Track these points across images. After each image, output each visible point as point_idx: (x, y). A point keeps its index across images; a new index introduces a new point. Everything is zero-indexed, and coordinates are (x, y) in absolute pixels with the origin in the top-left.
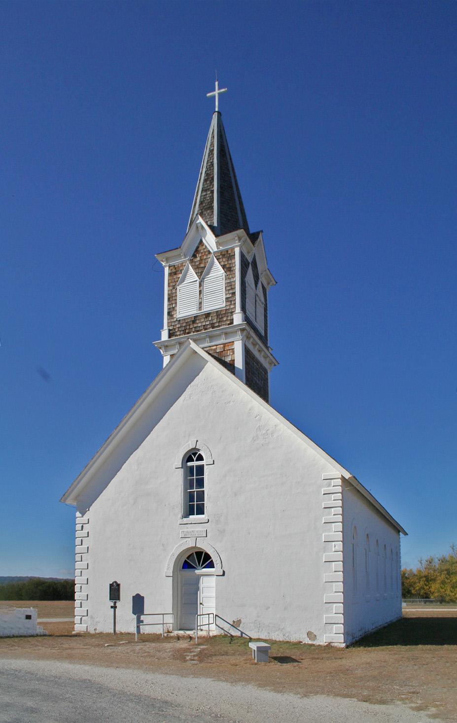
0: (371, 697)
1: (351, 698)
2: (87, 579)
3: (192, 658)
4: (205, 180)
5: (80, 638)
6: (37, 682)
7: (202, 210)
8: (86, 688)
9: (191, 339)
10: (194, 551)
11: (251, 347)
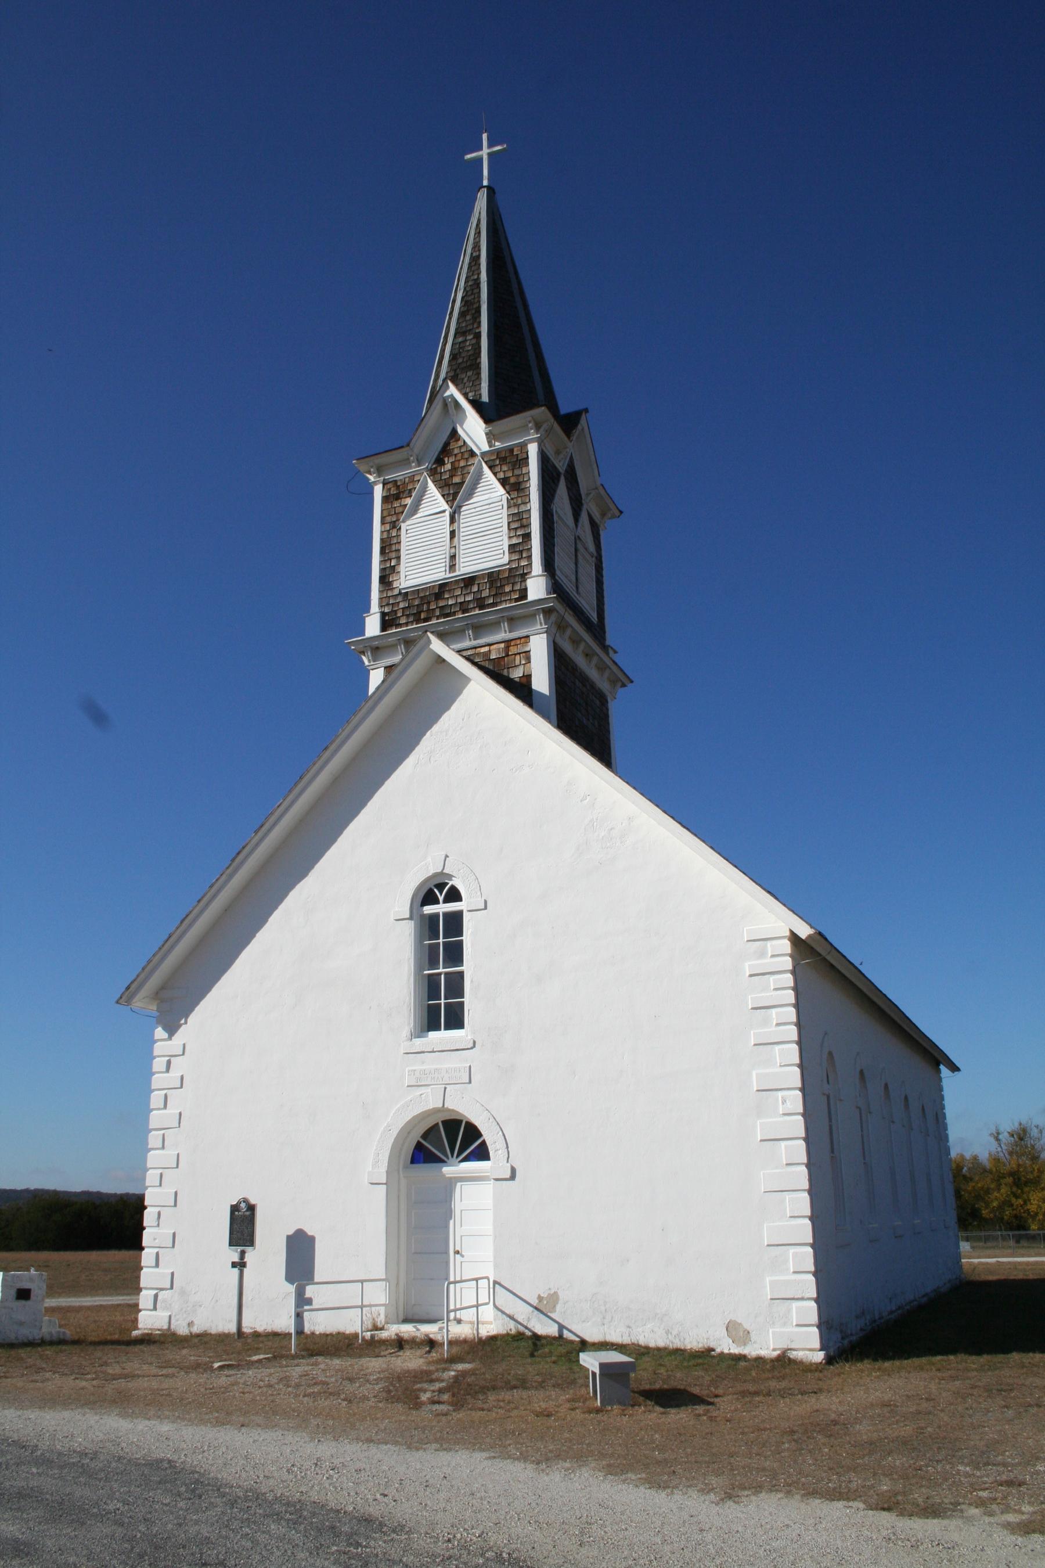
0: (900, 1498)
1: (848, 1499)
2: (176, 1193)
3: (436, 1398)
4: (462, 314)
5: (152, 1347)
6: (34, 1470)
7: (455, 370)
8: (160, 1483)
9: (432, 633)
10: (439, 1119)
11: (567, 647)
